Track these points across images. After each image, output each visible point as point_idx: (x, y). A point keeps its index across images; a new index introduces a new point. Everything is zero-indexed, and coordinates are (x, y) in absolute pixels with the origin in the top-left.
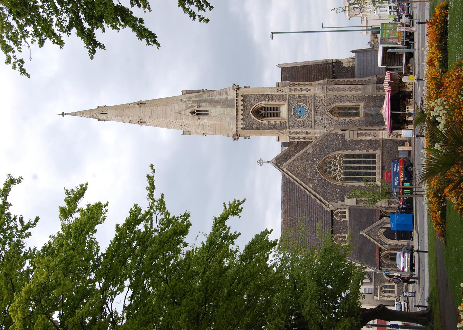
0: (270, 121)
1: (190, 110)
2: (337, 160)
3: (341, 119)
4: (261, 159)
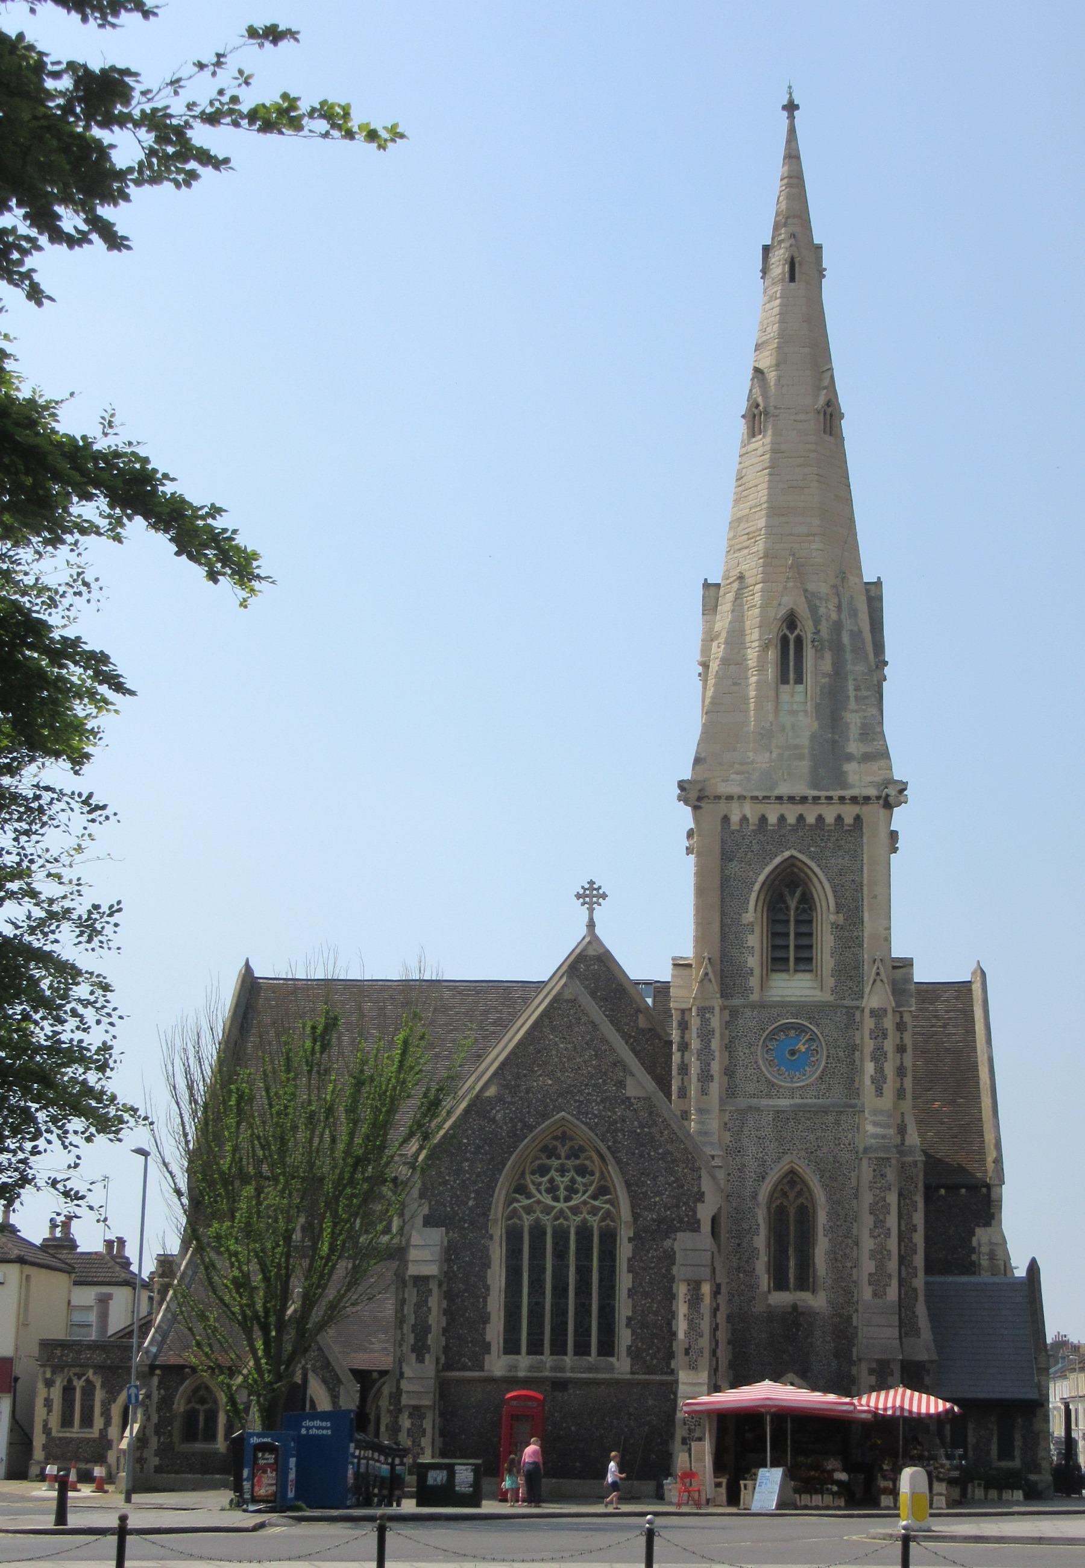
0: (757, 930)
1: (803, 611)
2: (595, 1197)
3: (761, 1215)
4: (604, 896)
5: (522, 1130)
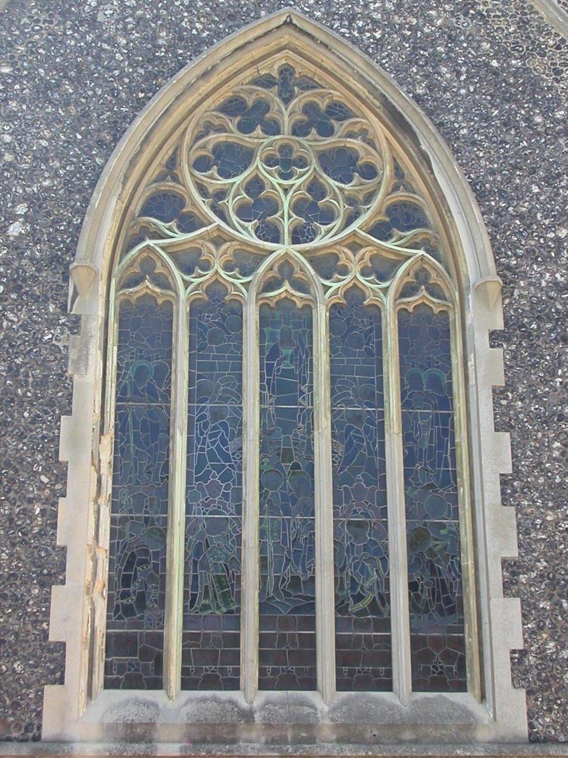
2: (381, 231)
5: (171, 47)
